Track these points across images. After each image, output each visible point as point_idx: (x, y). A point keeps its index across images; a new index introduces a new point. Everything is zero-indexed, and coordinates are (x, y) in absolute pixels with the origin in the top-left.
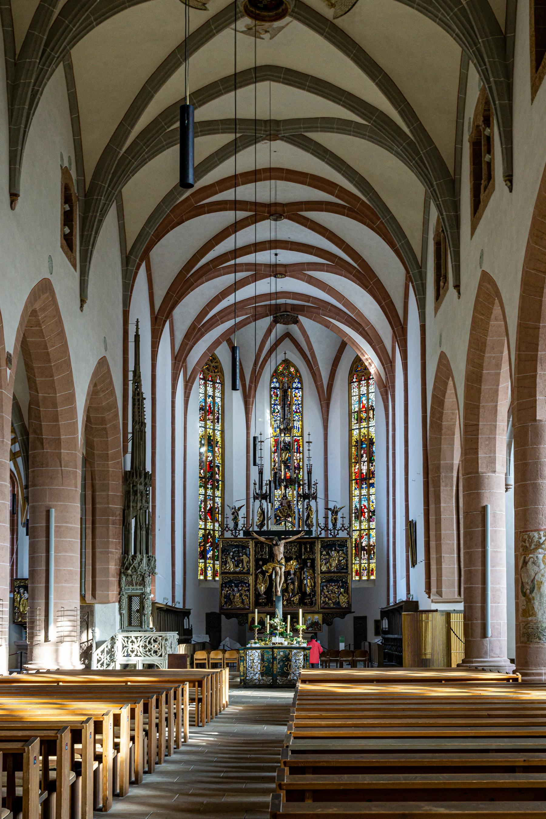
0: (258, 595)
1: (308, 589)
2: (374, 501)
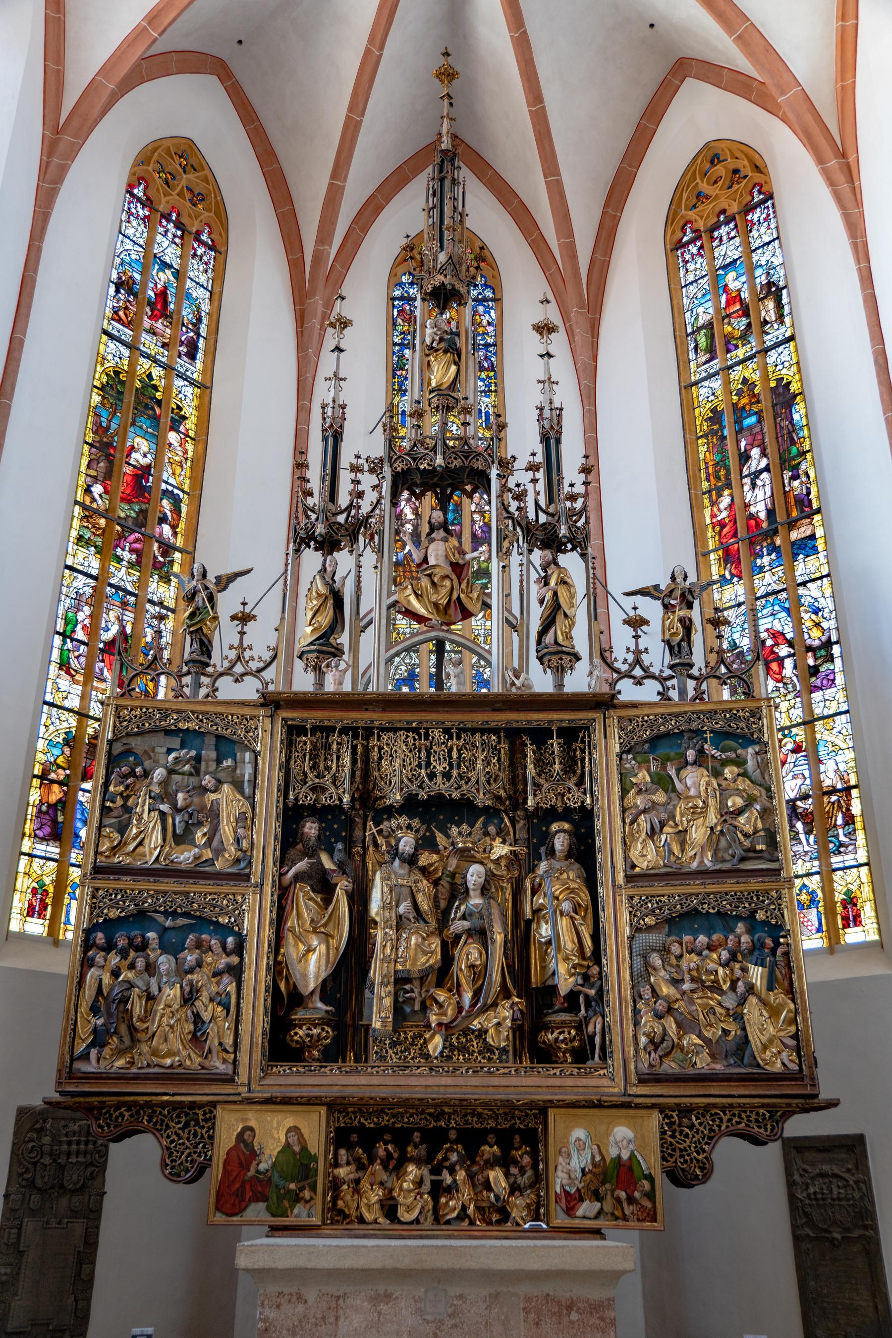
0: (285, 1001)
1: (562, 968)
2: (827, 604)
